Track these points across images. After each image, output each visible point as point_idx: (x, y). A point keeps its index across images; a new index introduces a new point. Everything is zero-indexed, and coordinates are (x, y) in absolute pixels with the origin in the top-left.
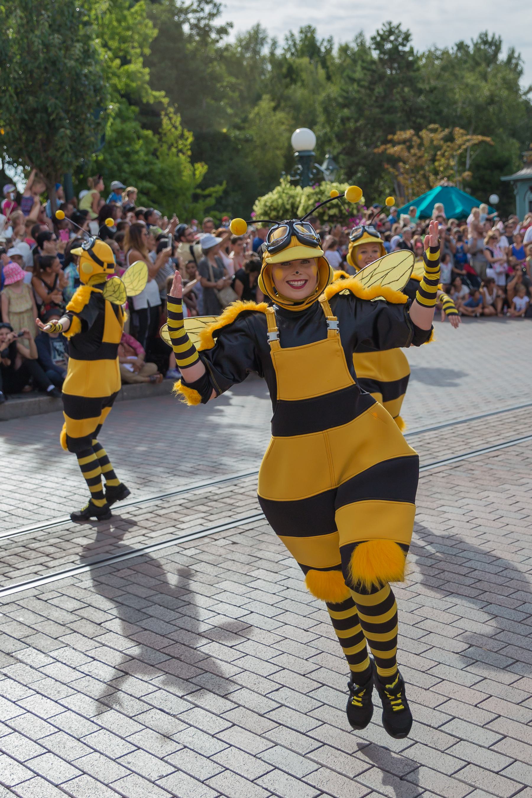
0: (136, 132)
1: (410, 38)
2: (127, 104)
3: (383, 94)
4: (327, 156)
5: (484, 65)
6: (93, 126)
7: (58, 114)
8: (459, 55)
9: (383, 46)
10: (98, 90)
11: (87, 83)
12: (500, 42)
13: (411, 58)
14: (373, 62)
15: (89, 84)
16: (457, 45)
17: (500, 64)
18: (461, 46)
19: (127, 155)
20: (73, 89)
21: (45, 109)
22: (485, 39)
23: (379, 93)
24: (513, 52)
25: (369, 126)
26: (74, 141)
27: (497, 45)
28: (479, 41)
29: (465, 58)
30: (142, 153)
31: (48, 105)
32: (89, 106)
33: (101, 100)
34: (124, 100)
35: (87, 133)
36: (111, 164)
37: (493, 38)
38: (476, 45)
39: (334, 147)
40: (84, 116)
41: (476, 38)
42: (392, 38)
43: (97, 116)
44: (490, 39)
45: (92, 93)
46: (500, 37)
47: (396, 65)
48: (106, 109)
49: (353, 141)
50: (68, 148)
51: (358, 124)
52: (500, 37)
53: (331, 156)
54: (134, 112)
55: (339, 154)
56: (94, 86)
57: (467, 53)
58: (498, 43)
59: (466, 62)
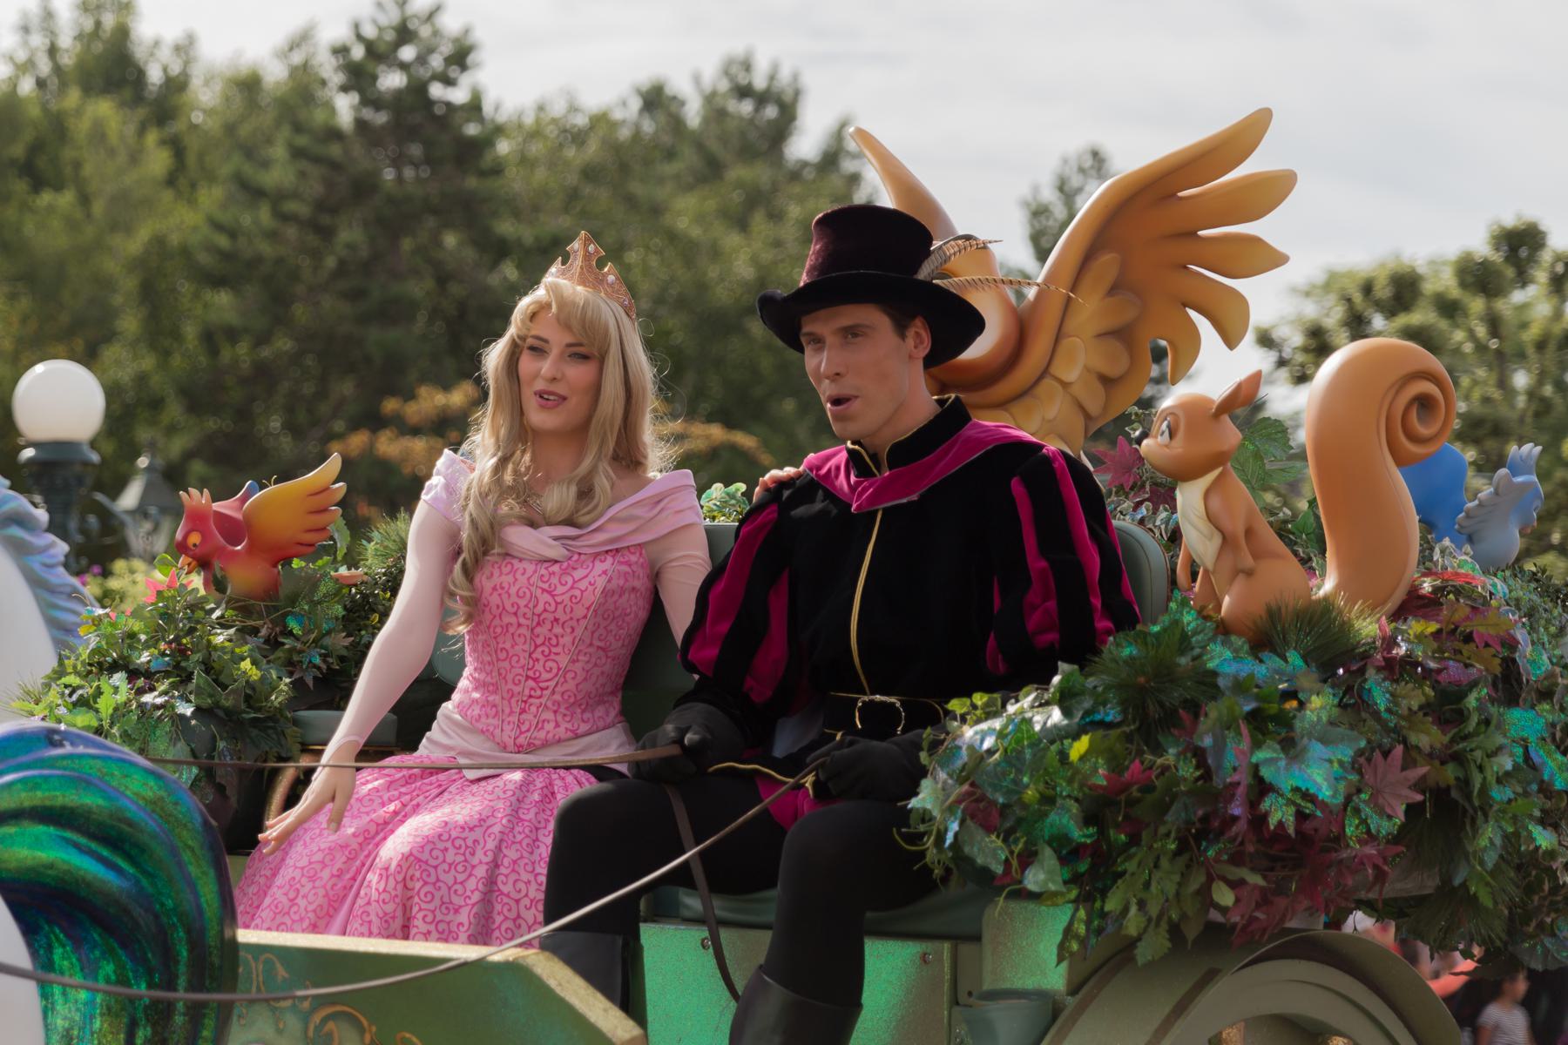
1: (470, 59)
3: (364, 253)
4: (143, 462)
8: (648, 126)
9: (374, 78)
12: (797, 93)
13: (472, 130)
14: (334, 134)
16: (639, 92)
18: (655, 99)
22: (743, 79)
23: (350, 246)
25: (309, 361)
27: (781, 108)
28: (724, 86)
29: (667, 139)
37: (772, 78)
38: (710, 99)
39: (172, 430)
42: (407, 53)
44: (760, 83)
46: (796, 77)
47: (416, 150)
49: (244, 414)
51: (266, 352)
52: (796, 77)
53: (160, 462)
55: (189, 455)
57: (677, 124)
58: (787, 98)
59: (671, 155)
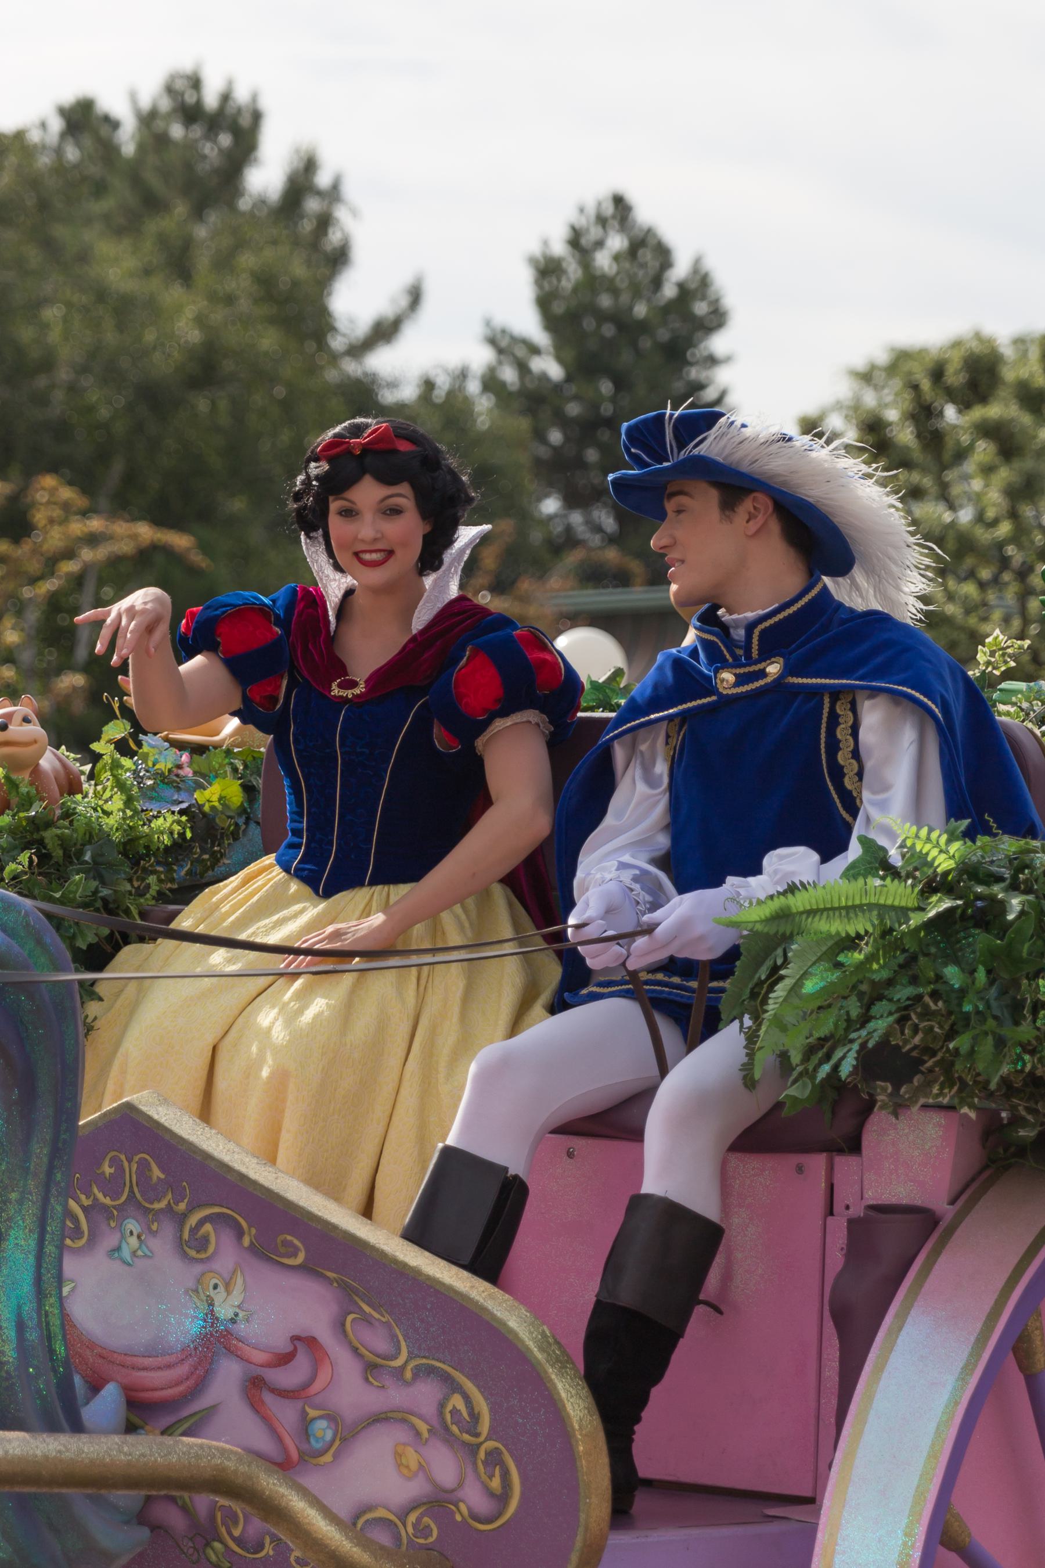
5: (181, 209)
12: (257, 117)
17: (251, 214)
18: (81, 118)
22: (190, 98)
24: (309, 165)
28: (165, 105)
41: (150, 91)
44: (211, 99)
58: (245, 121)
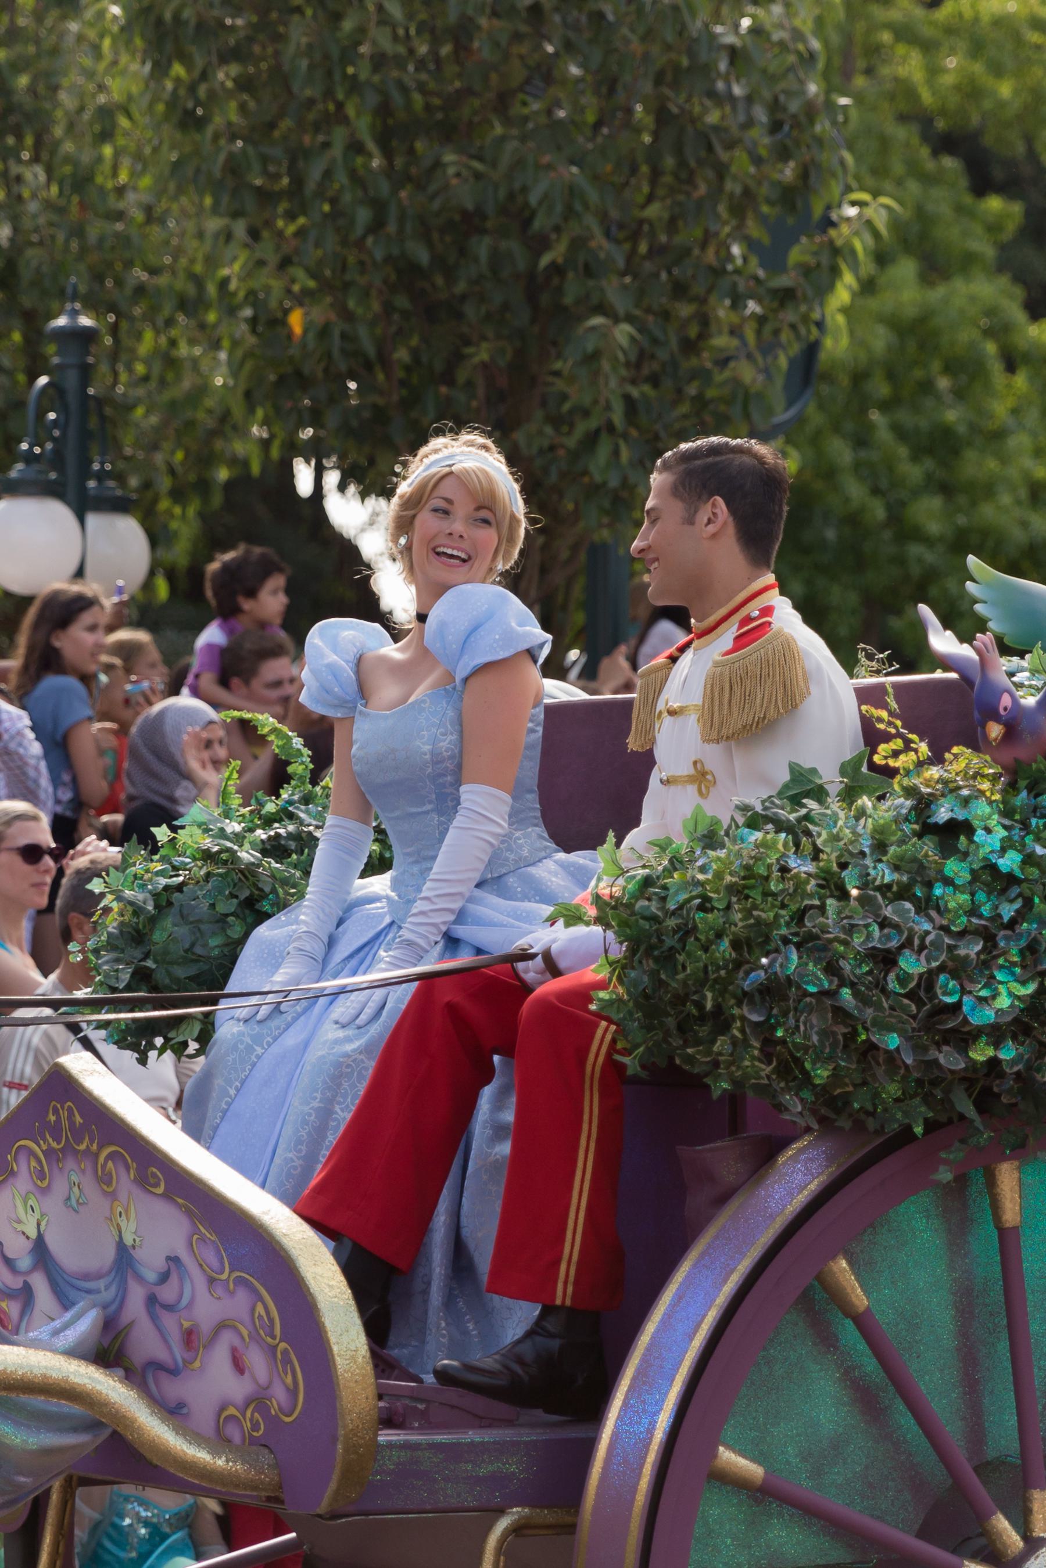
0: (999, 330)
2: (963, 182)
6: (752, 306)
7: (578, 244)
10: (790, 128)
11: (737, 90)
15: (749, 99)
19: (940, 446)
20: (662, 116)
21: (518, 216)
26: (655, 381)
30: (1020, 441)
31: (533, 199)
32: (743, 204)
33: (804, 174)
34: (949, 163)
35: (721, 341)
36: (855, 490)
40: (710, 256)
43: (773, 257)
45: (761, 138)
48: (828, 223)
50: (618, 417)
54: (993, 228)
56: (775, 106)
